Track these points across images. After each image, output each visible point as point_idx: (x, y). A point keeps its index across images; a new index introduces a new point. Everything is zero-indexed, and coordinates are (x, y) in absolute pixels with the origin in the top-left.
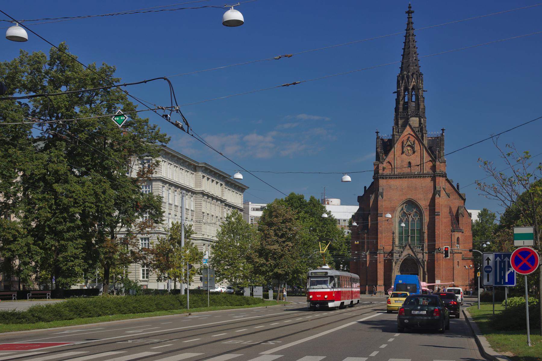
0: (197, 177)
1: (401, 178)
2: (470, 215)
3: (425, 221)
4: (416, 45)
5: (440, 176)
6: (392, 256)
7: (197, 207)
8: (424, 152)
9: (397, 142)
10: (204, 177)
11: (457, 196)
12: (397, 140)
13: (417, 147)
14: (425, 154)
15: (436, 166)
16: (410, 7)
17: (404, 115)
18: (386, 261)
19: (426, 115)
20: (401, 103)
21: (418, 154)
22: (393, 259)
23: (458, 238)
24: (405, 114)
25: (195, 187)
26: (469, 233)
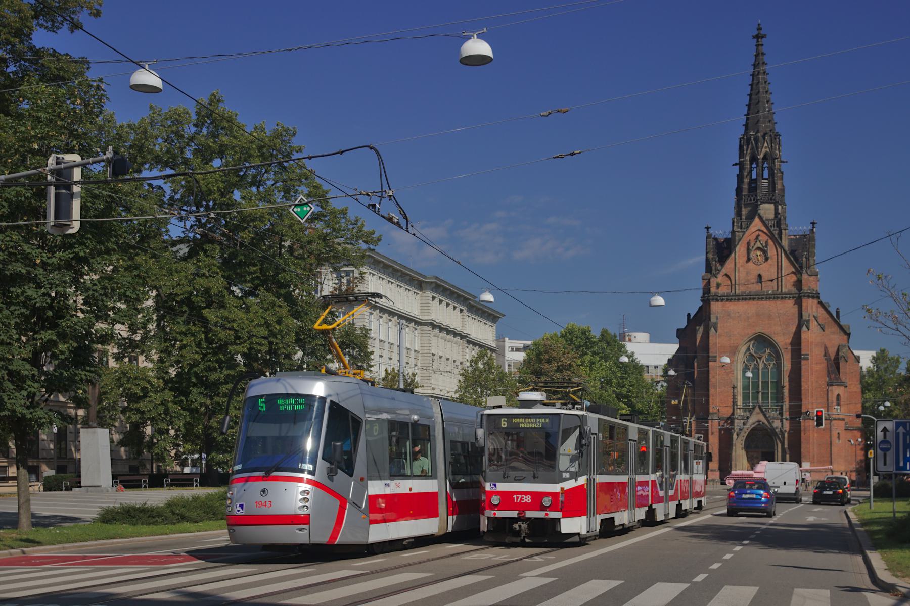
0: (424, 298)
1: (746, 299)
2: (858, 359)
3: (785, 369)
4: (770, 88)
5: (809, 297)
6: (732, 423)
7: (423, 345)
8: (783, 259)
9: (740, 243)
10: (434, 298)
11: (836, 328)
12: (740, 240)
13: (772, 251)
14: (785, 262)
15: (803, 281)
16: (759, 29)
17: (751, 200)
18: (723, 432)
19: (787, 199)
20: (746, 180)
21: (773, 261)
22: (733, 429)
23: (838, 395)
24: (752, 198)
25: (420, 314)
26: (856, 388)
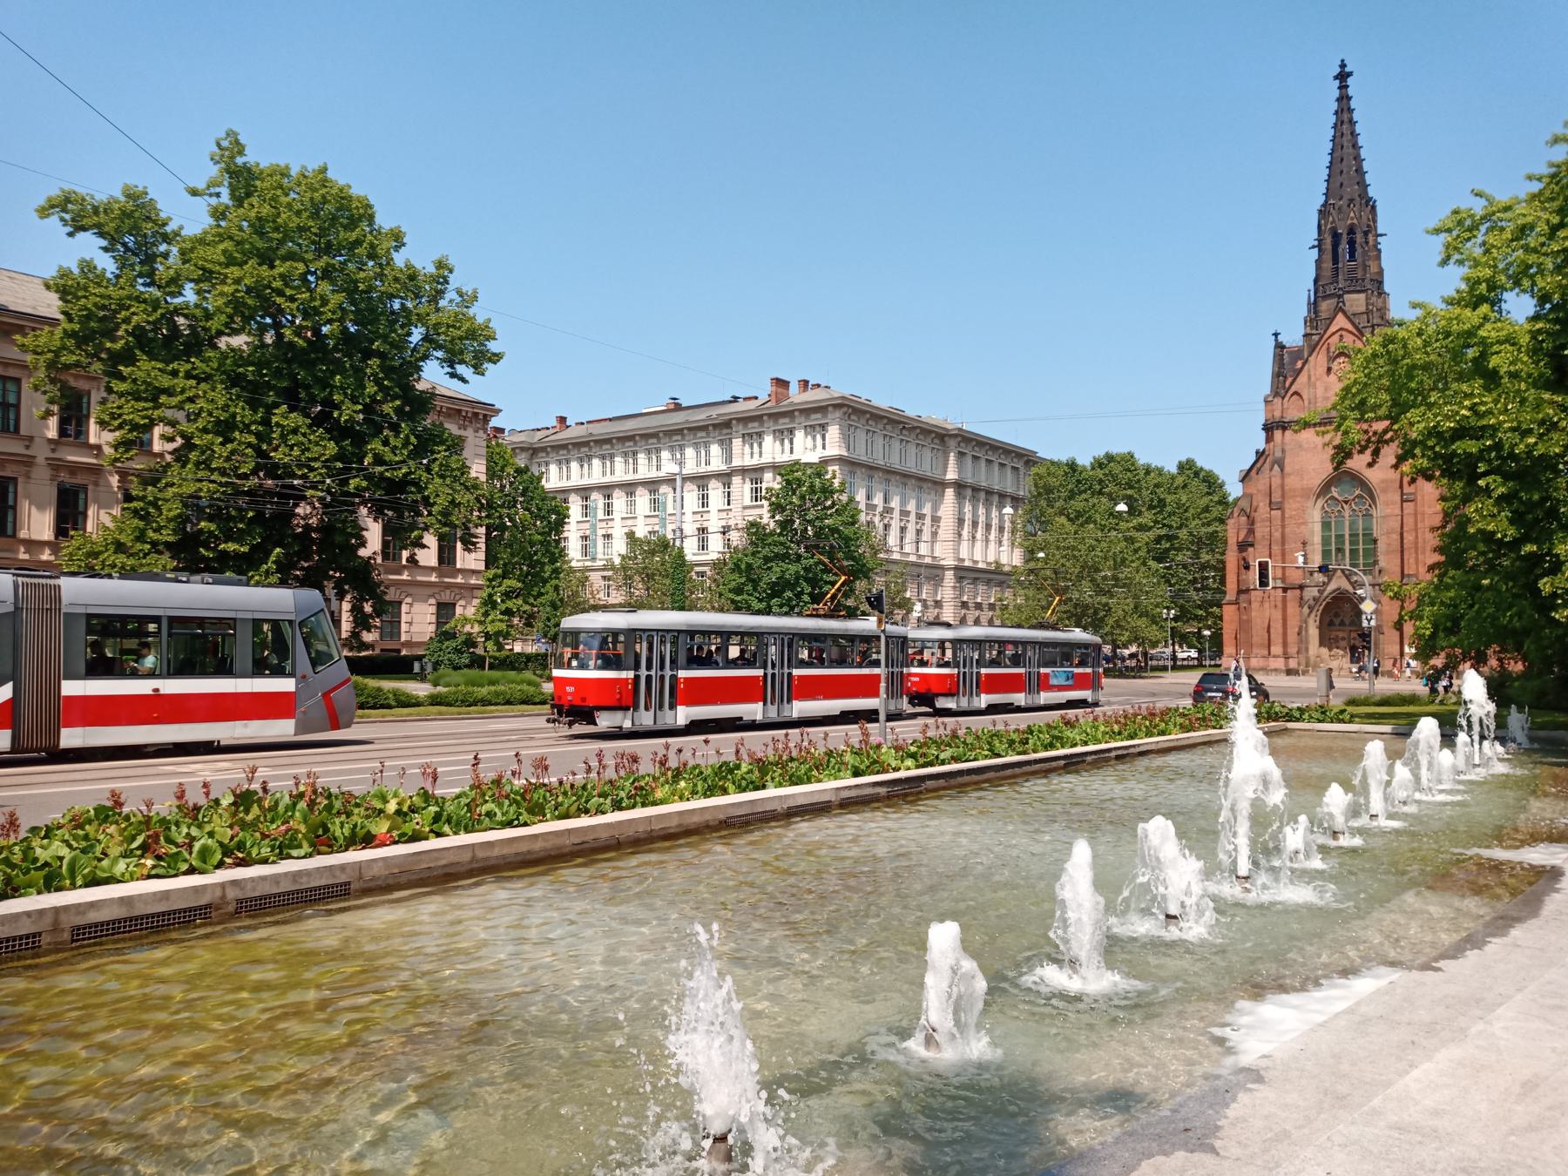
16: (1343, 66)
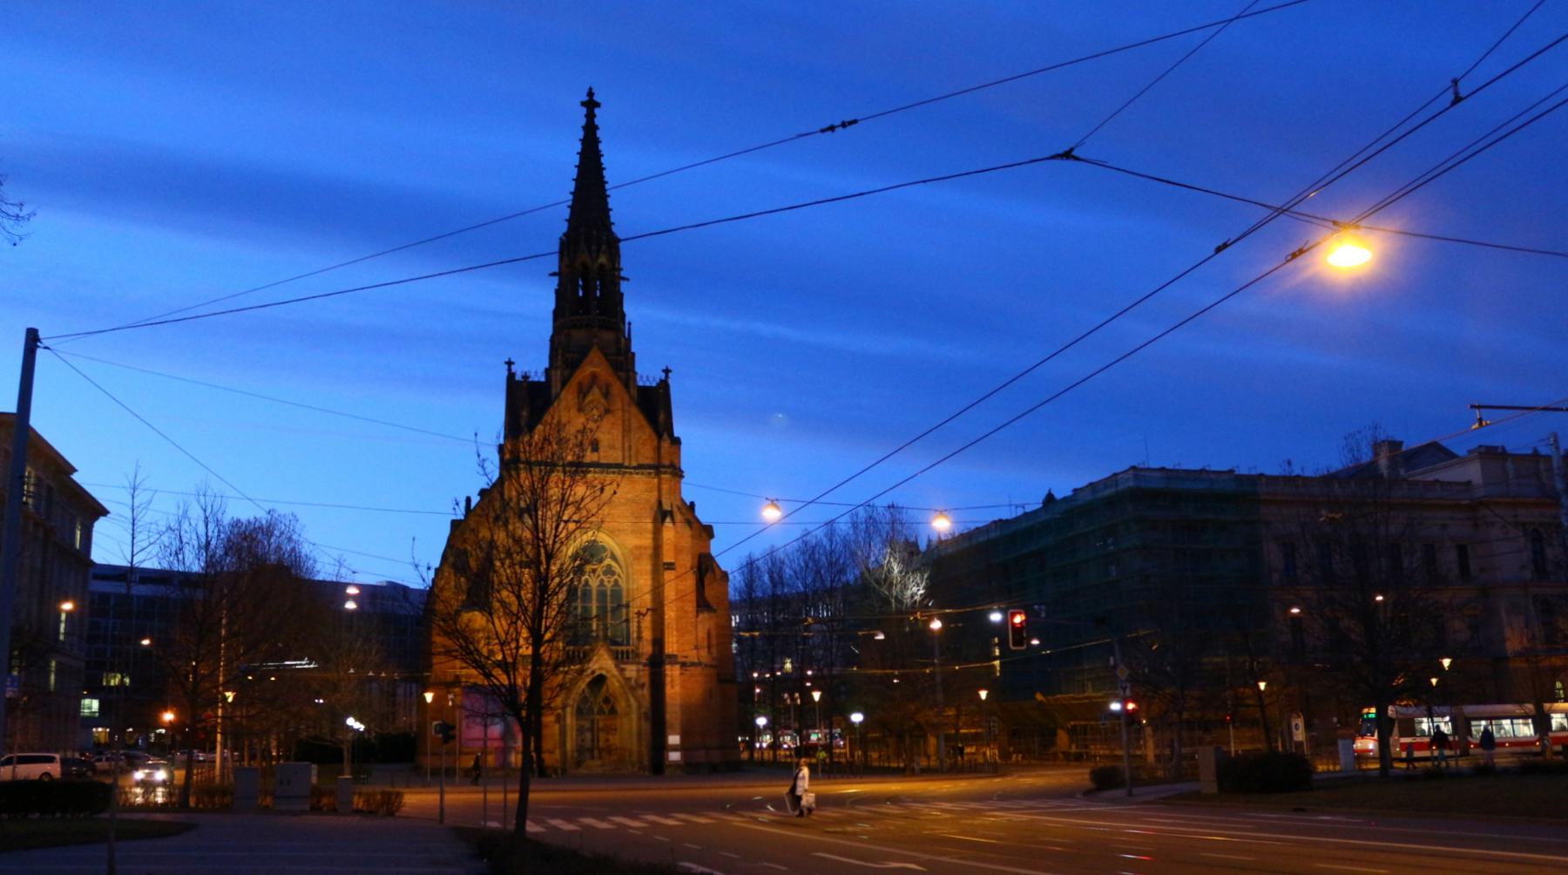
16: (591, 94)
